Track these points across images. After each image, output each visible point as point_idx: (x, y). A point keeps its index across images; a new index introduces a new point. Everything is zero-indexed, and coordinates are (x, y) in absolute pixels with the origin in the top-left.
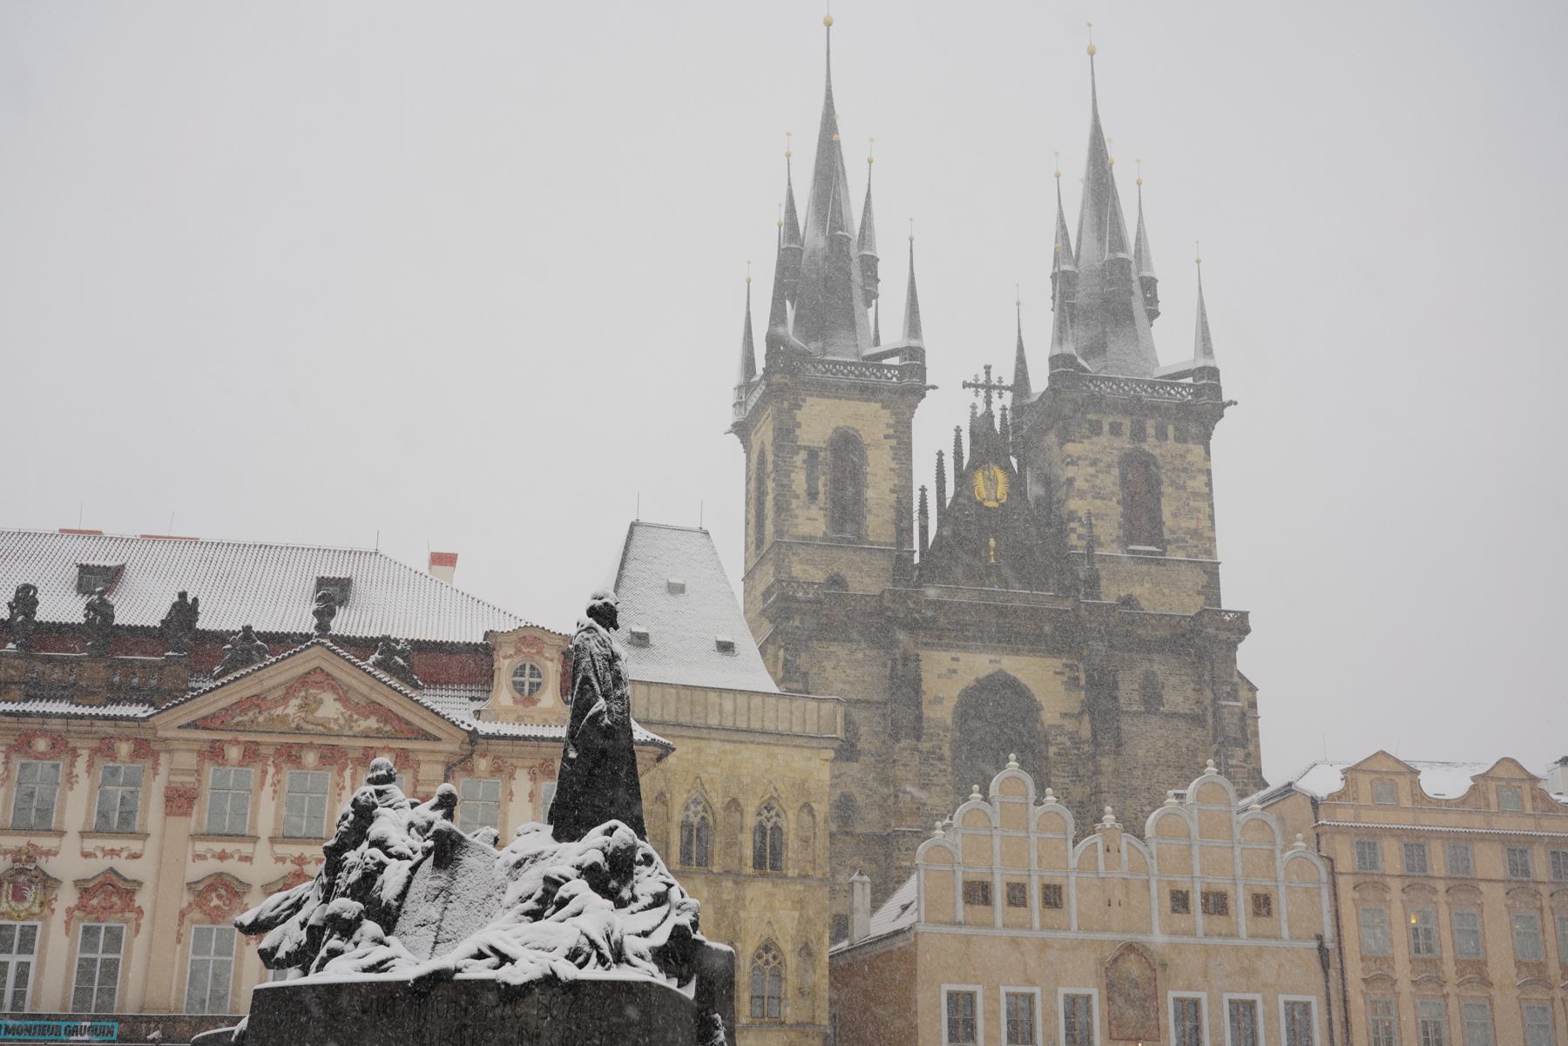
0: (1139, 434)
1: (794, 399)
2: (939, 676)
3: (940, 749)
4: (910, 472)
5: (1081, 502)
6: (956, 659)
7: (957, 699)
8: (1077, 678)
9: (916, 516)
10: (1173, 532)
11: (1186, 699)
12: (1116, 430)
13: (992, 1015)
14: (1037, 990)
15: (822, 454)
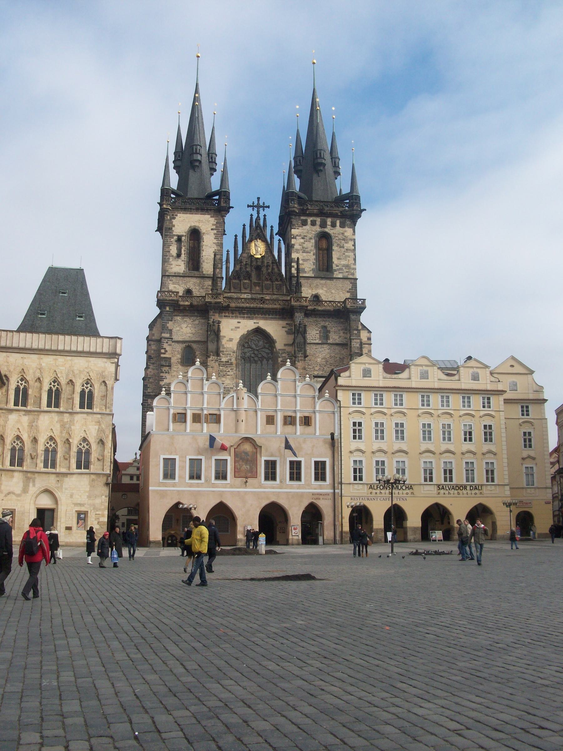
0: (324, 225)
1: (172, 215)
2: (232, 330)
3: (231, 360)
4: (222, 244)
5: (297, 254)
6: (239, 322)
7: (239, 339)
8: (292, 329)
9: (224, 263)
10: (337, 266)
11: (340, 337)
12: (313, 223)
13: (182, 468)
14: (203, 458)
15: (183, 238)
